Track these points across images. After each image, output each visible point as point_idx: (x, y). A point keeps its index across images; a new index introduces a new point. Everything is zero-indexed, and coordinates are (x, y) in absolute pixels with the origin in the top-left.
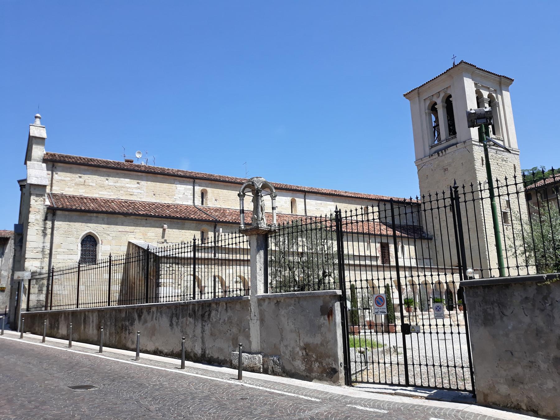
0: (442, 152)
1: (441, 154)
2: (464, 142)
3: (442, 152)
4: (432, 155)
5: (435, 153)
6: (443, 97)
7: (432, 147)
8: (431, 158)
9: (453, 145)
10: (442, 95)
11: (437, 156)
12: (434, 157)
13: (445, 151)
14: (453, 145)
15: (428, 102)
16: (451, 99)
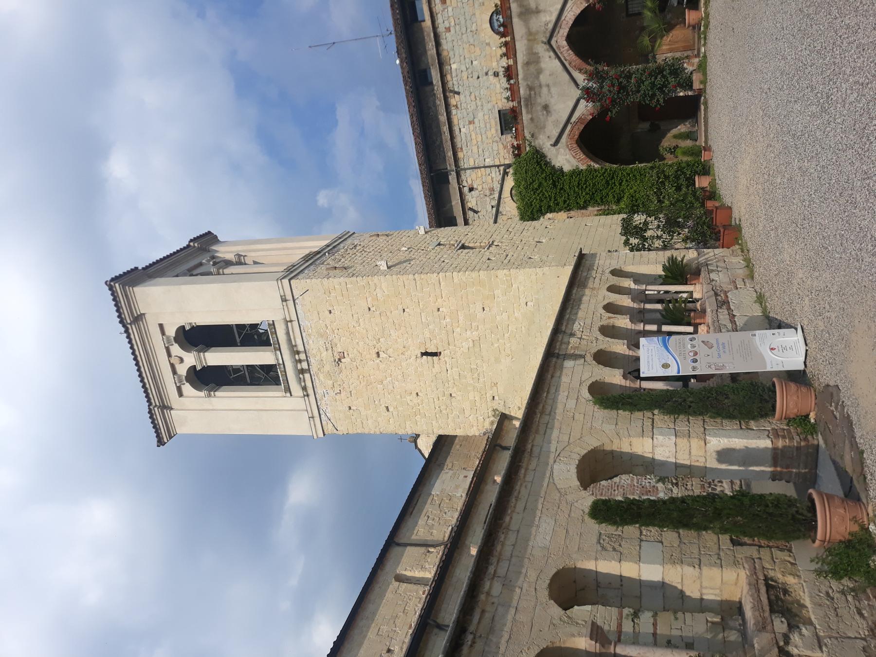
0: (300, 361)
1: (305, 365)
2: (284, 300)
3: (300, 361)
4: (304, 388)
5: (299, 380)
6: (182, 347)
7: (288, 390)
8: (310, 391)
9: (288, 334)
10: (176, 349)
11: (307, 376)
12: (309, 384)
13: (298, 353)
14: (288, 334)
15: (187, 388)
16: (187, 328)
